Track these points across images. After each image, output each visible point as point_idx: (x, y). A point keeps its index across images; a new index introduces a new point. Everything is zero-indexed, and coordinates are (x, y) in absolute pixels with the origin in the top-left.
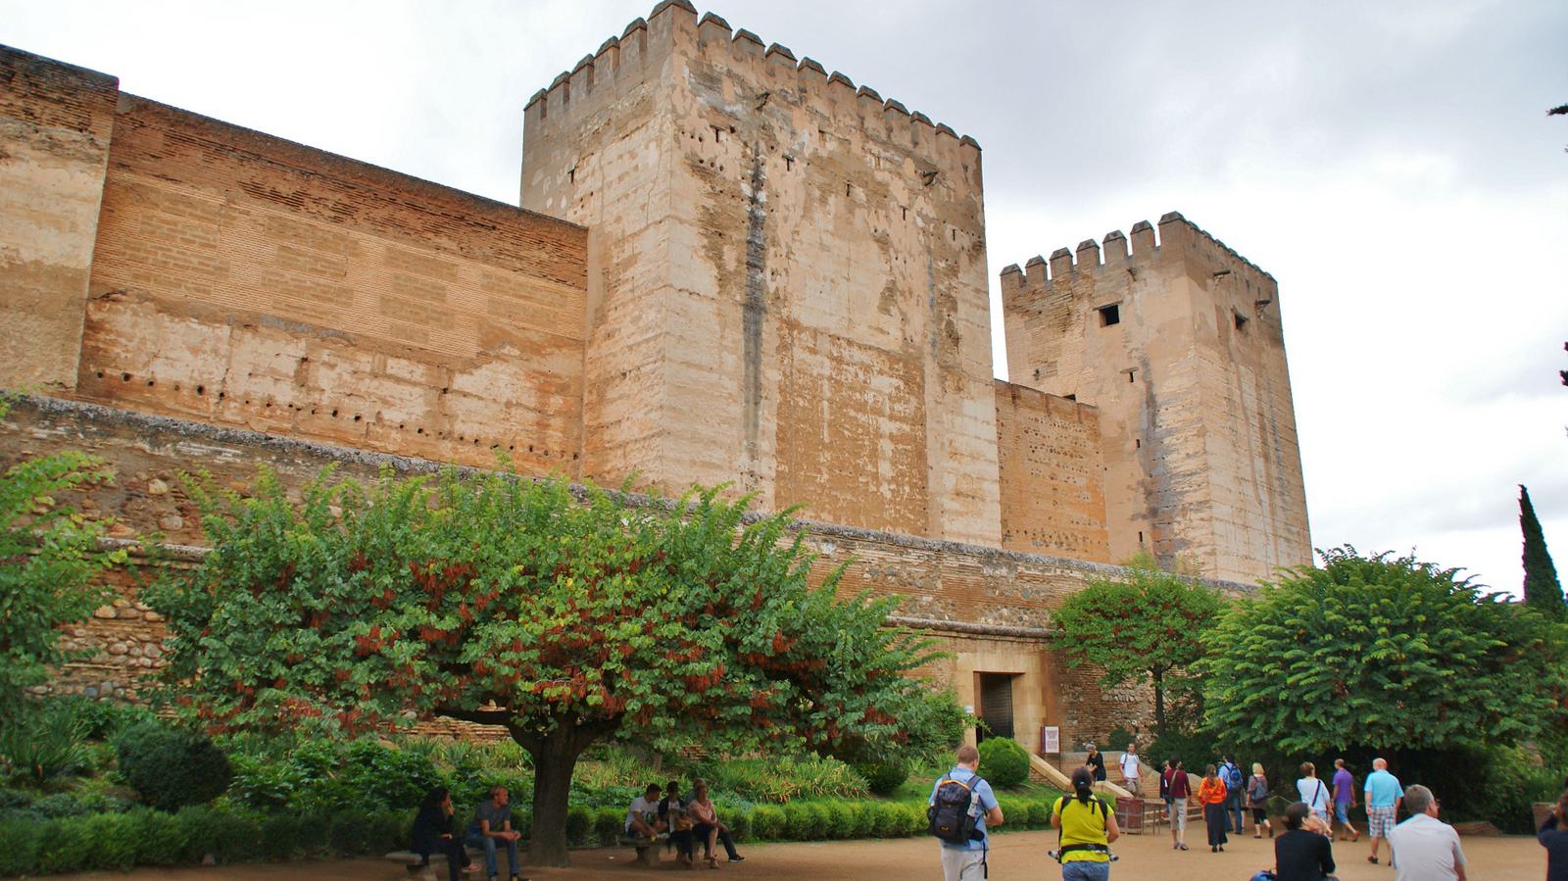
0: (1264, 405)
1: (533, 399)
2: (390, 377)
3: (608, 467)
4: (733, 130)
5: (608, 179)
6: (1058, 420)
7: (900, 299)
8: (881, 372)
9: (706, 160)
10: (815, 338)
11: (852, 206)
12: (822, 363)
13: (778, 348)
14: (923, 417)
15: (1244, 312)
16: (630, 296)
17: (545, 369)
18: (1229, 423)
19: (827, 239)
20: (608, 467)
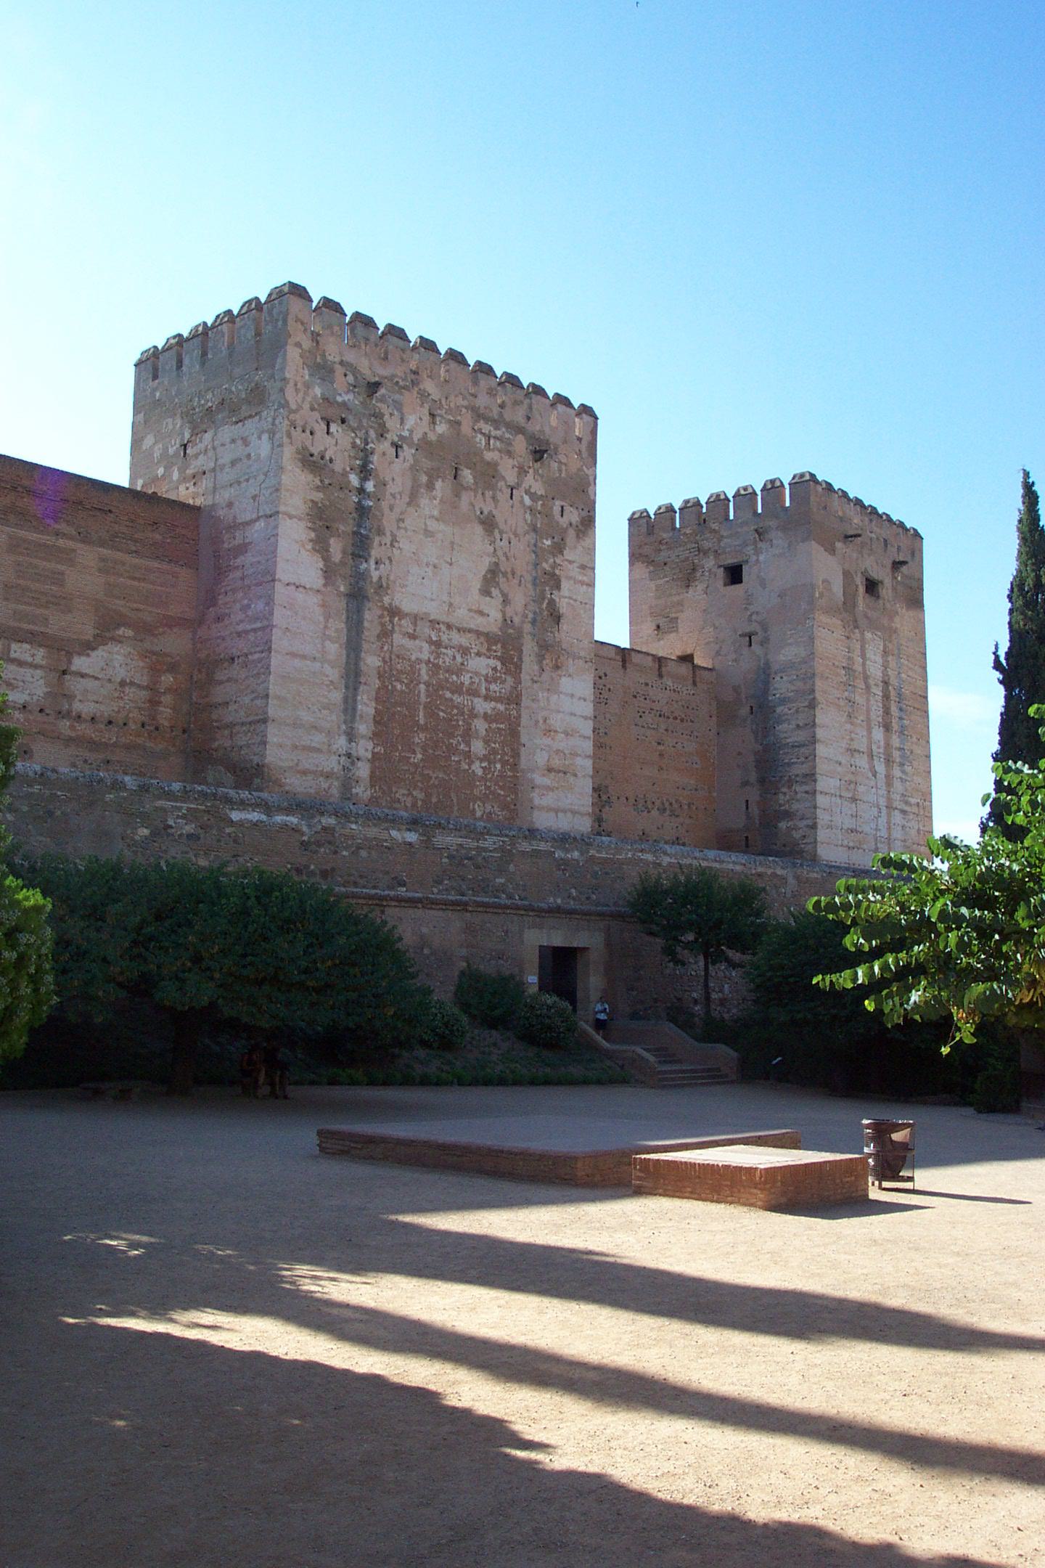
0: (890, 672)
1: (145, 678)
2: (13, 661)
3: (216, 745)
4: (343, 421)
5: (221, 461)
6: (670, 683)
7: (502, 580)
8: (478, 654)
9: (316, 454)
10: (415, 625)
11: (458, 488)
12: (421, 647)
13: (378, 636)
14: (519, 696)
15: (876, 574)
16: (239, 583)
17: (158, 649)
18: (846, 693)
19: (433, 525)
20: (216, 745)
